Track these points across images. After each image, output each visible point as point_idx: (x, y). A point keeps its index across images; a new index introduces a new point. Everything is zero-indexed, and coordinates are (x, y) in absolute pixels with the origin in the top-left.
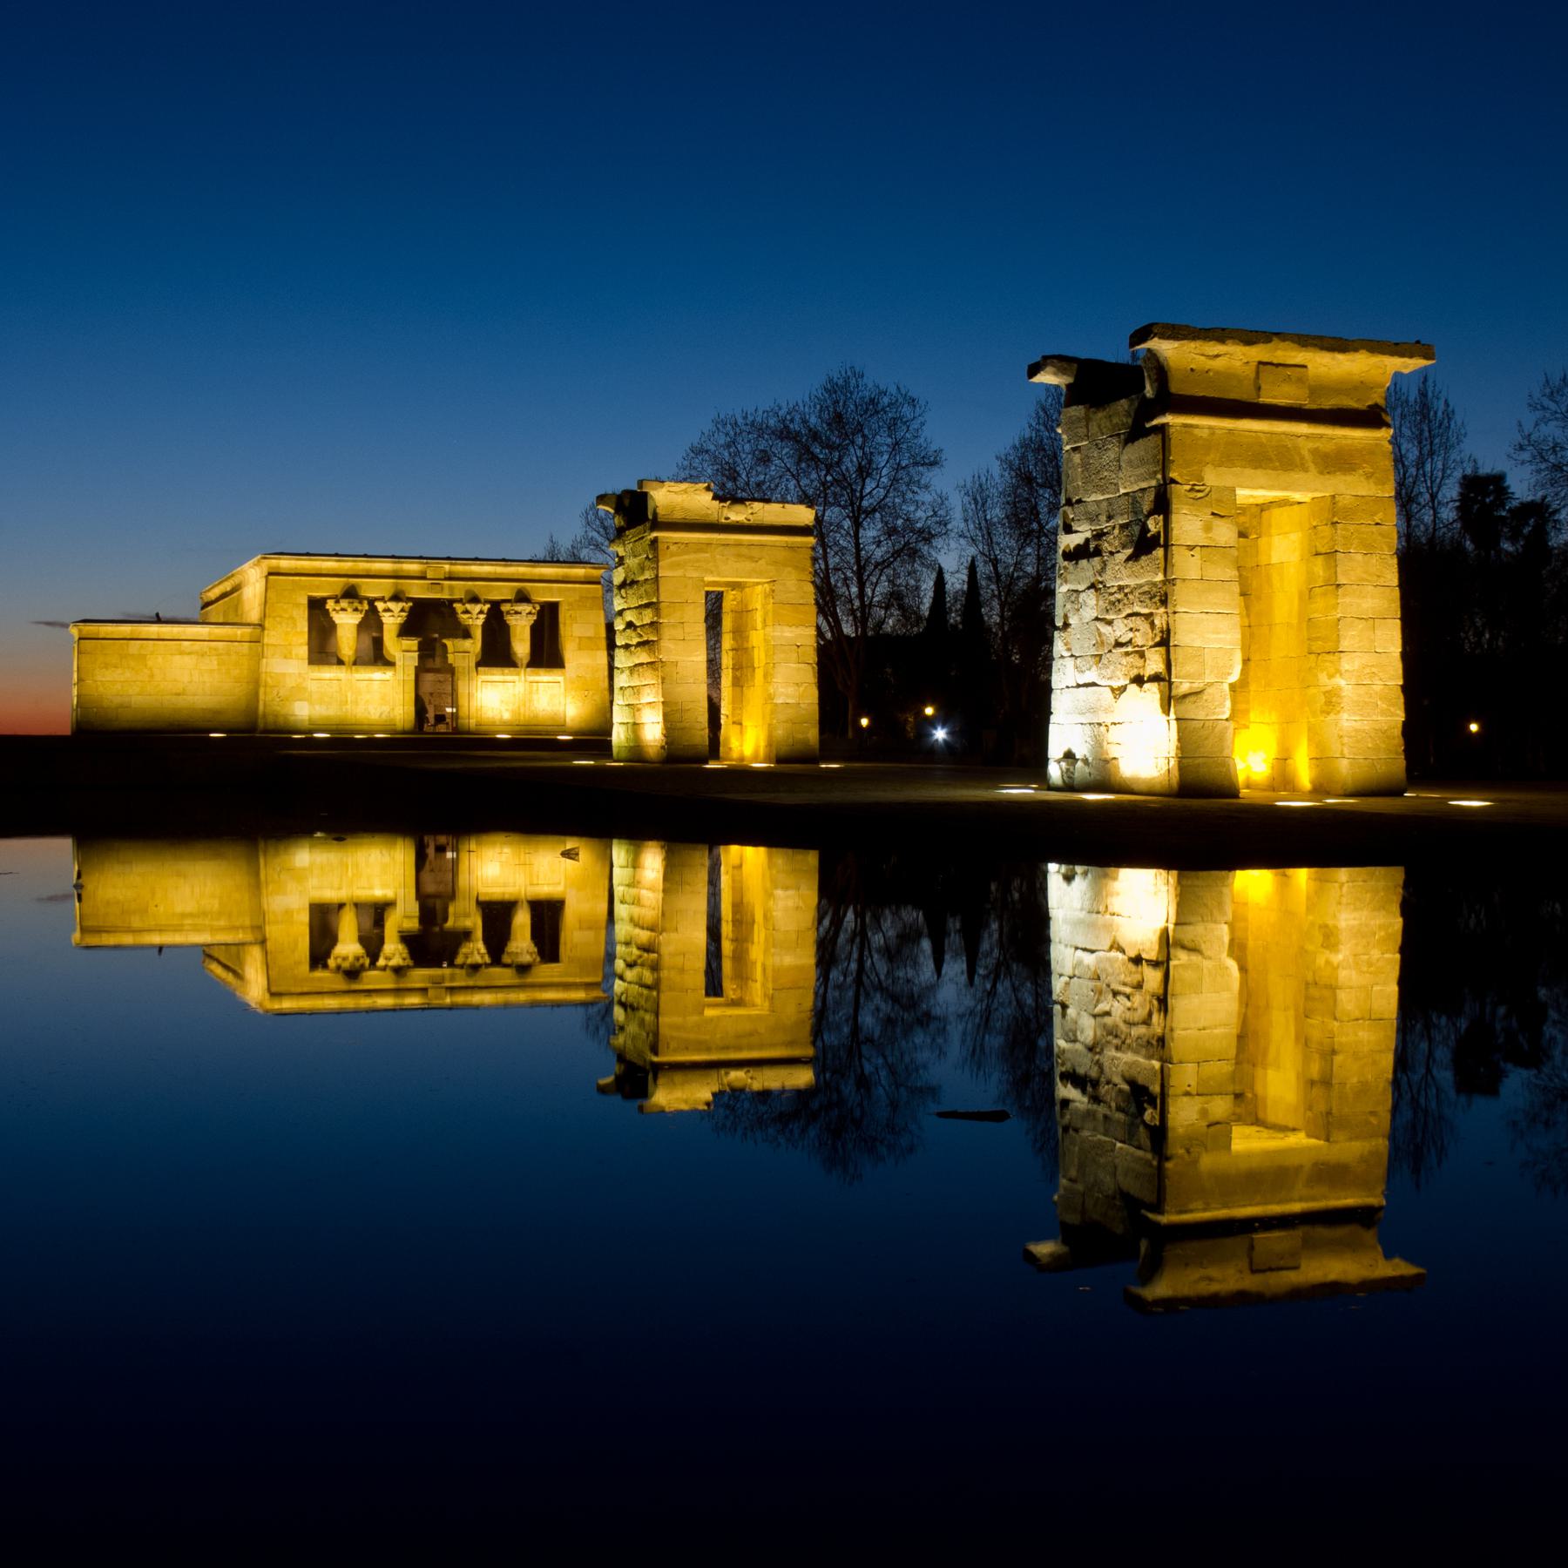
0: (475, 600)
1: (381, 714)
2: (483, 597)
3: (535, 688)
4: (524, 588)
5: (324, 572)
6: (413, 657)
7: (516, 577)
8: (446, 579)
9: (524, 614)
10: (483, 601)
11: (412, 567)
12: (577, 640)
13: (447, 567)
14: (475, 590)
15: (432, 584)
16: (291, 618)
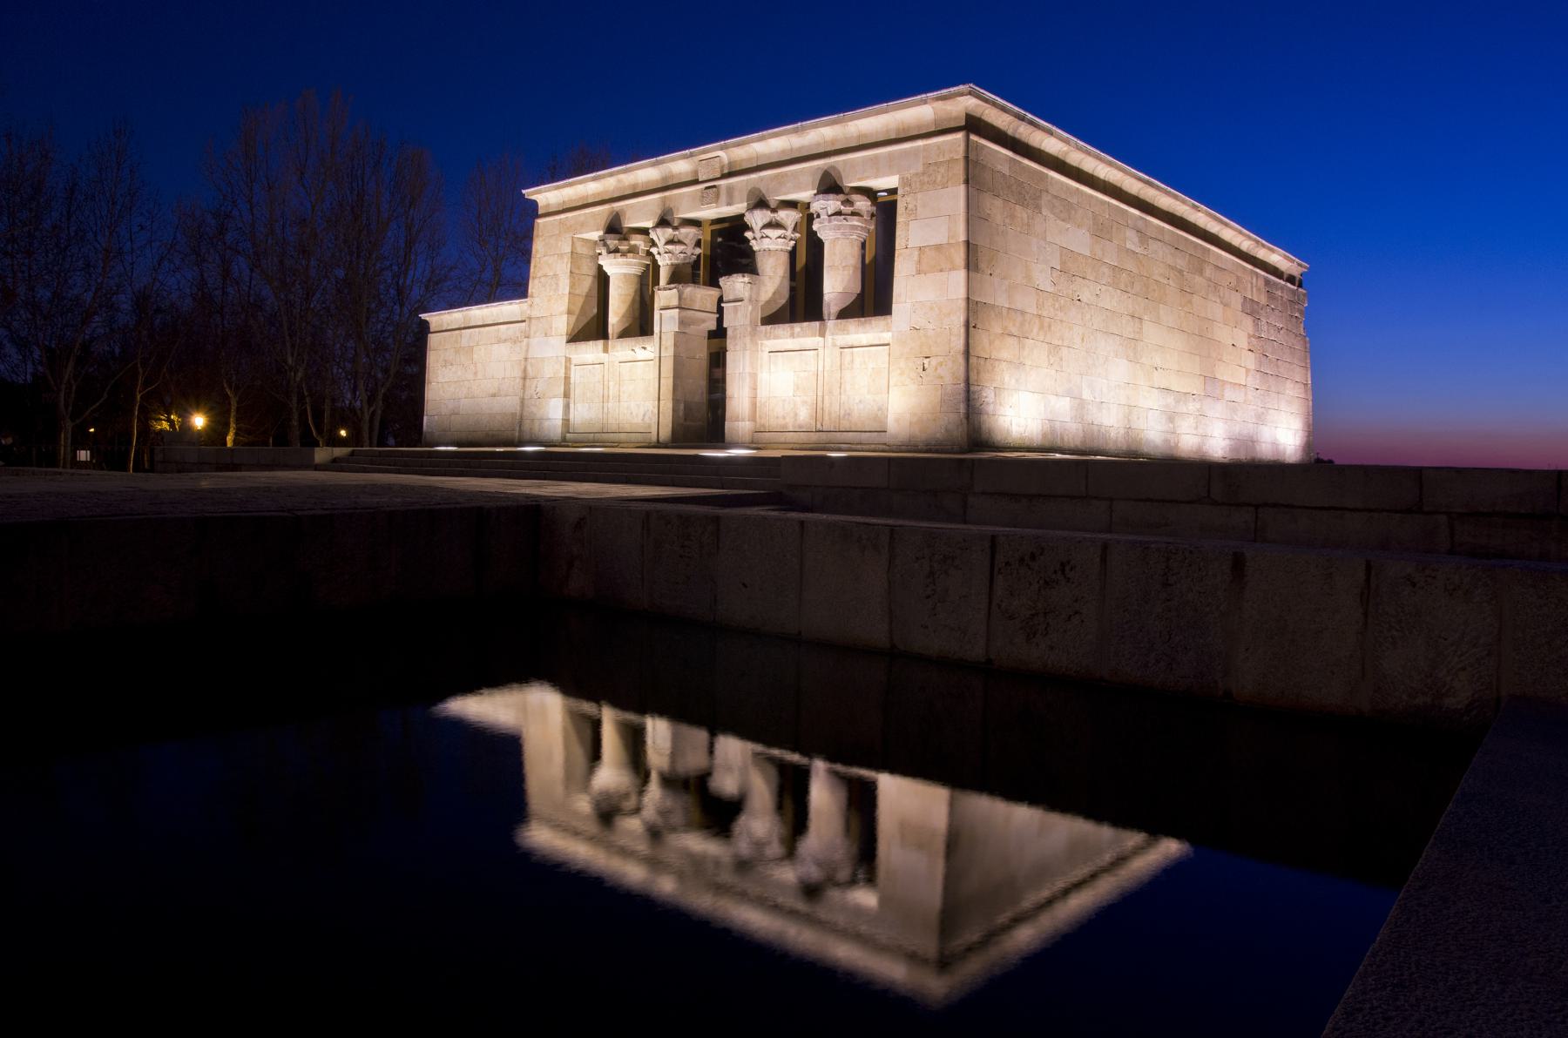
0: (761, 203)
1: (644, 415)
2: (774, 199)
3: (847, 359)
4: (833, 168)
5: (590, 201)
6: (672, 318)
7: (822, 150)
8: (724, 176)
9: (824, 216)
10: (773, 205)
11: (679, 165)
12: (916, 253)
13: (720, 153)
14: (764, 192)
15: (707, 188)
16: (555, 275)
